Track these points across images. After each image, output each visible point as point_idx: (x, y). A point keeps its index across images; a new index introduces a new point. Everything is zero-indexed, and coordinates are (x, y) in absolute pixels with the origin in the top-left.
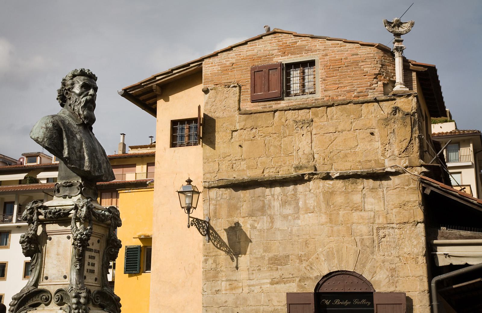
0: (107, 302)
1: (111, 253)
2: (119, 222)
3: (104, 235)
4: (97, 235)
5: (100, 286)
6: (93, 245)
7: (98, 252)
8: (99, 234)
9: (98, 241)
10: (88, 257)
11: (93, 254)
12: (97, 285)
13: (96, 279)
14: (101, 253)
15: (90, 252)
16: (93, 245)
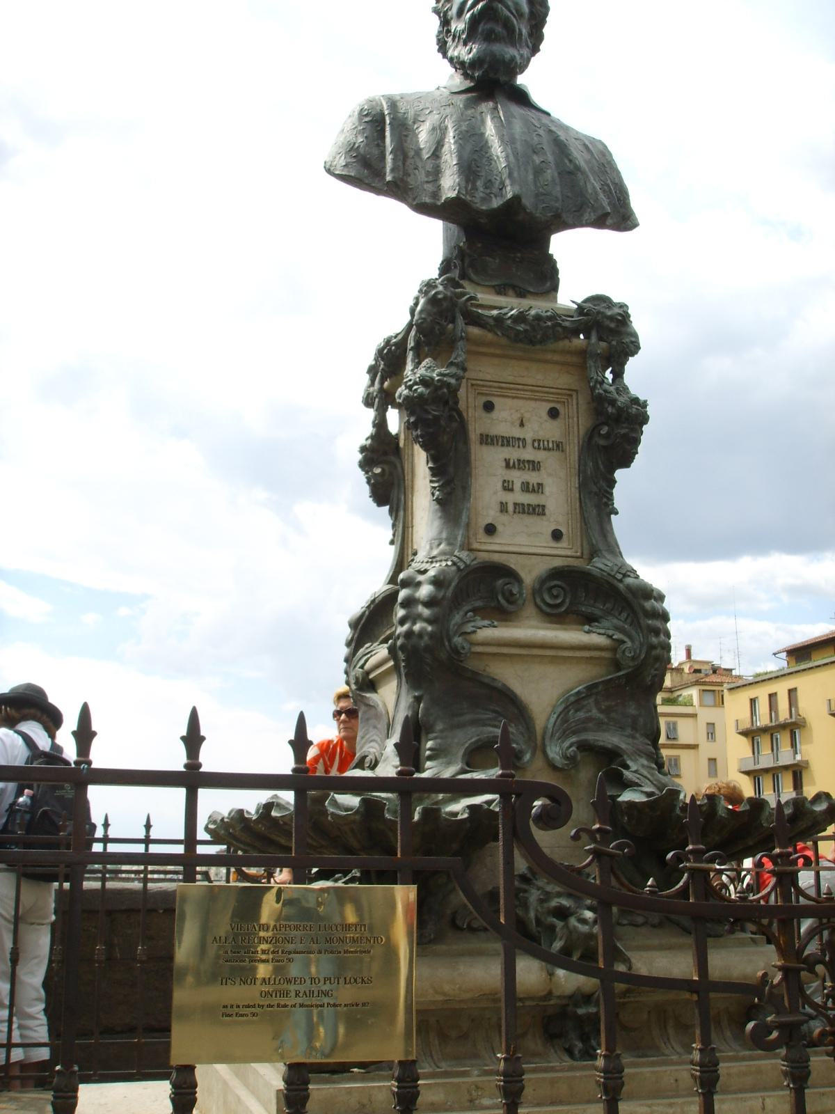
0: (607, 606)
1: (602, 442)
2: (627, 340)
3: (576, 391)
4: (532, 391)
5: (579, 554)
6: (522, 425)
7: (559, 446)
8: (552, 390)
9: (553, 413)
10: (504, 464)
11: (528, 454)
12: (569, 553)
13: (557, 535)
14: (573, 450)
15: (506, 449)
16: (522, 425)
